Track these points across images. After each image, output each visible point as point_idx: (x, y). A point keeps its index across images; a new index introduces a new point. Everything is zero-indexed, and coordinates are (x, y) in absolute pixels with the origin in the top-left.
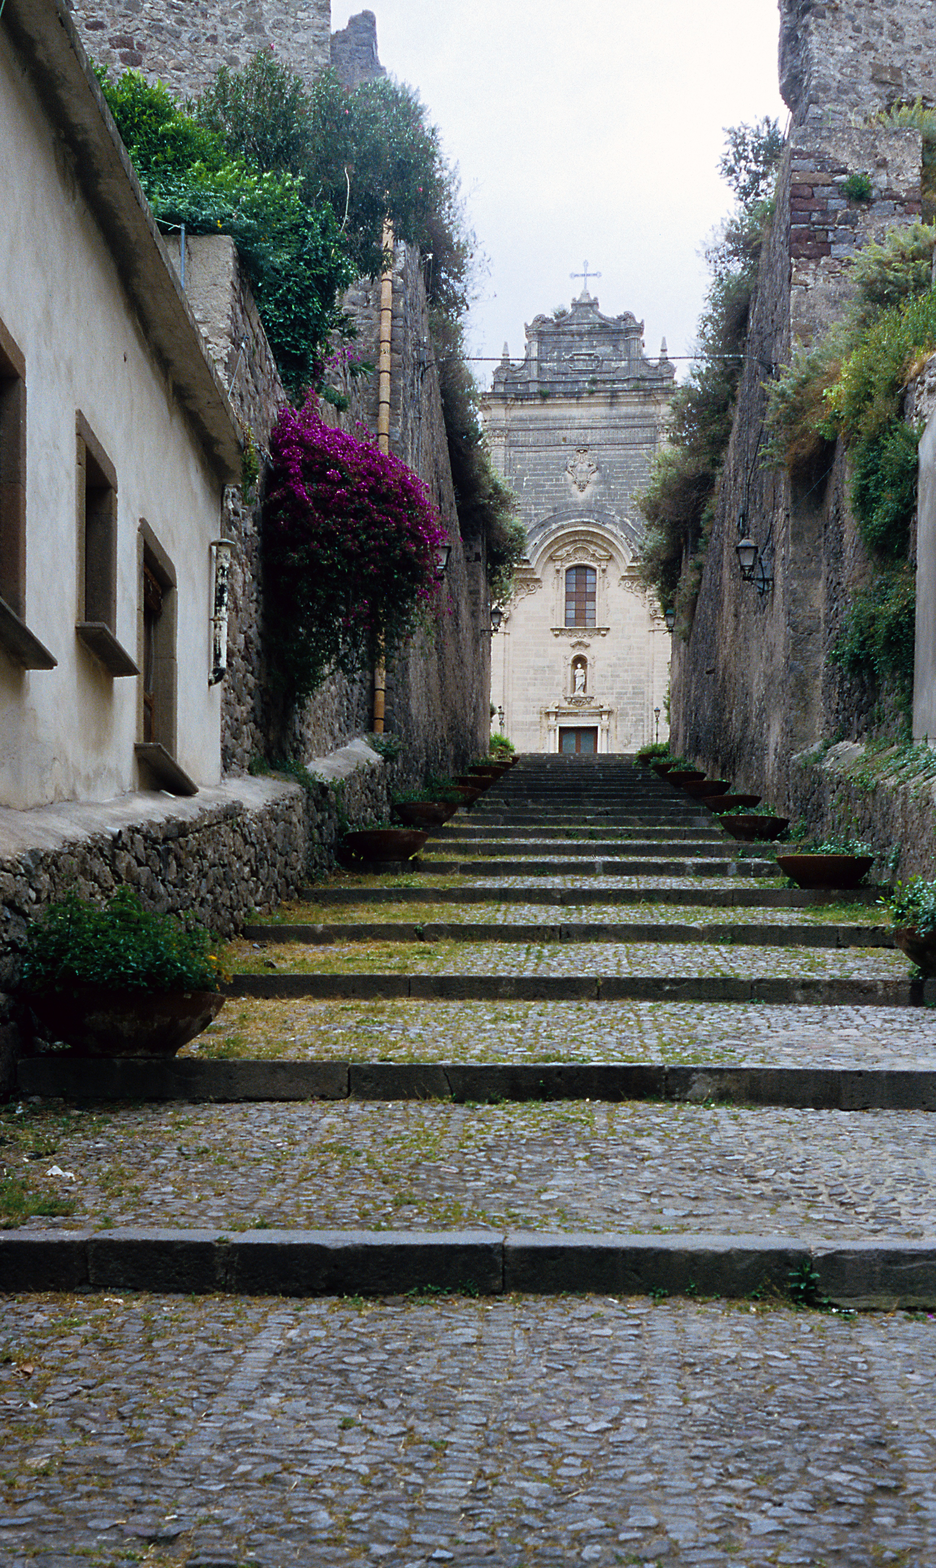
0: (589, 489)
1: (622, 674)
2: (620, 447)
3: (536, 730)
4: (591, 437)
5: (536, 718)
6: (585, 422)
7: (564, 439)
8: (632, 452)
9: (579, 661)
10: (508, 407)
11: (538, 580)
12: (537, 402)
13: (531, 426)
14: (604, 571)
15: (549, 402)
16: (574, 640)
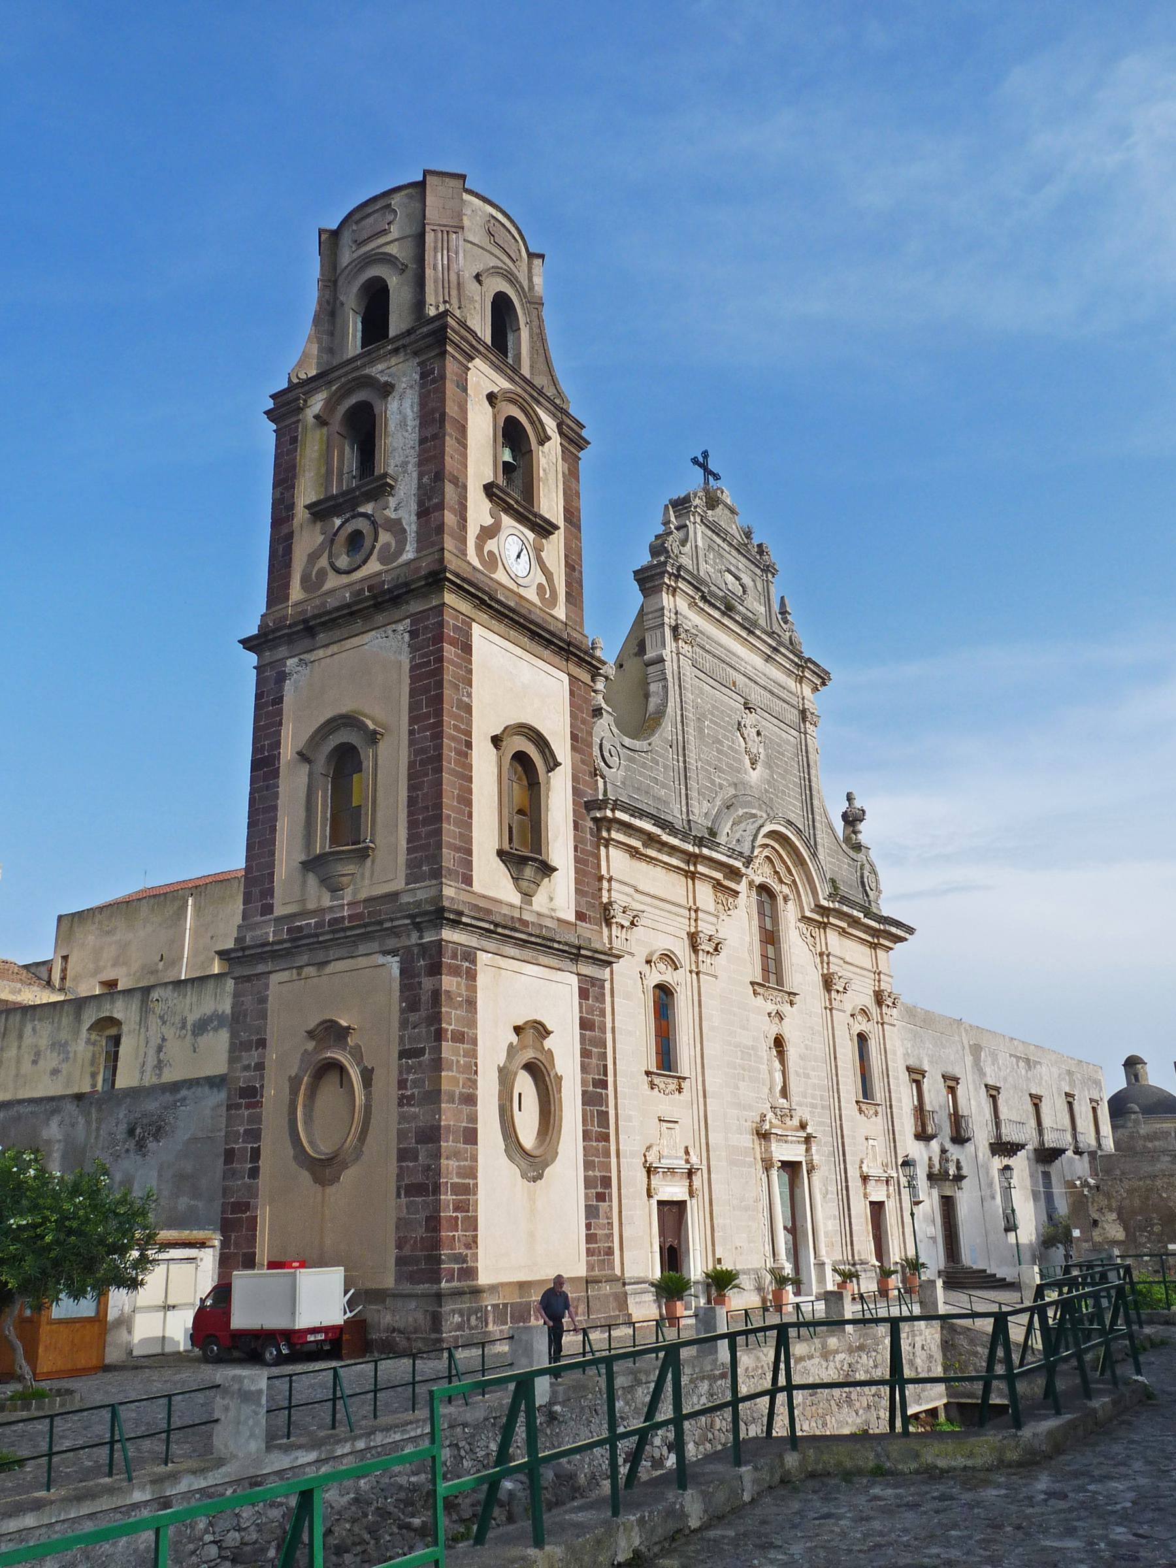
0: (759, 767)
1: (811, 1073)
2: (776, 721)
3: (750, 1166)
4: (757, 696)
5: (748, 1140)
6: (750, 672)
7: (734, 683)
8: (784, 735)
9: (779, 1042)
10: (693, 604)
11: (736, 893)
12: (717, 614)
13: (707, 647)
14: (786, 899)
15: (726, 621)
16: (771, 1007)
